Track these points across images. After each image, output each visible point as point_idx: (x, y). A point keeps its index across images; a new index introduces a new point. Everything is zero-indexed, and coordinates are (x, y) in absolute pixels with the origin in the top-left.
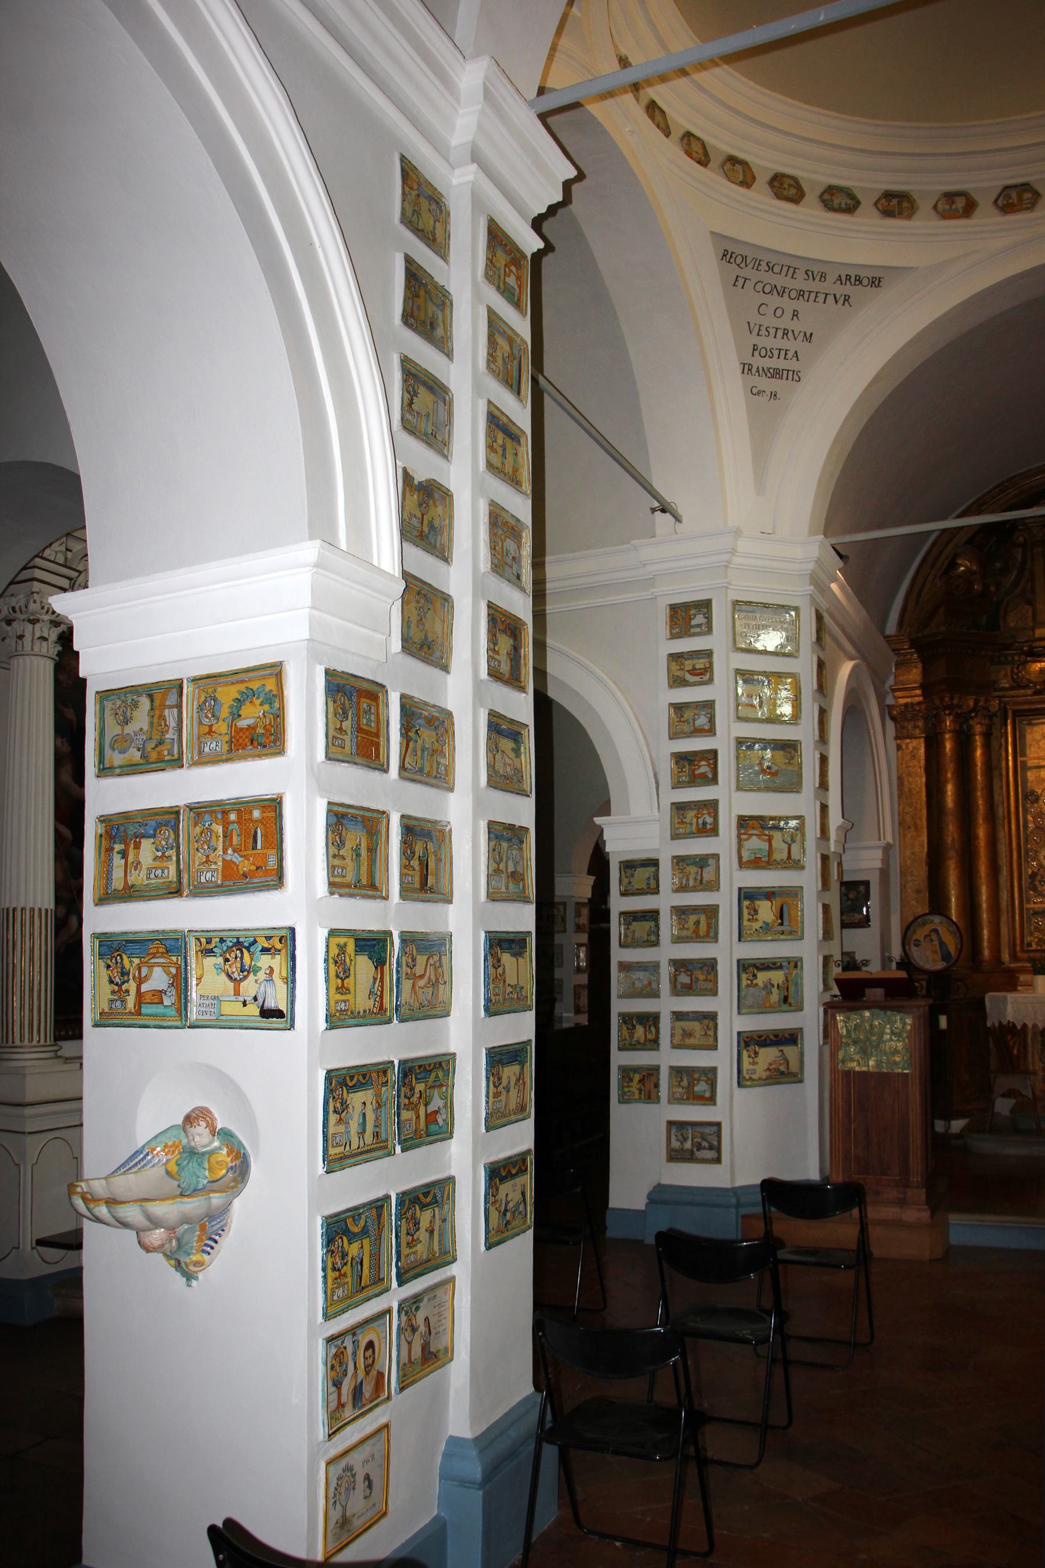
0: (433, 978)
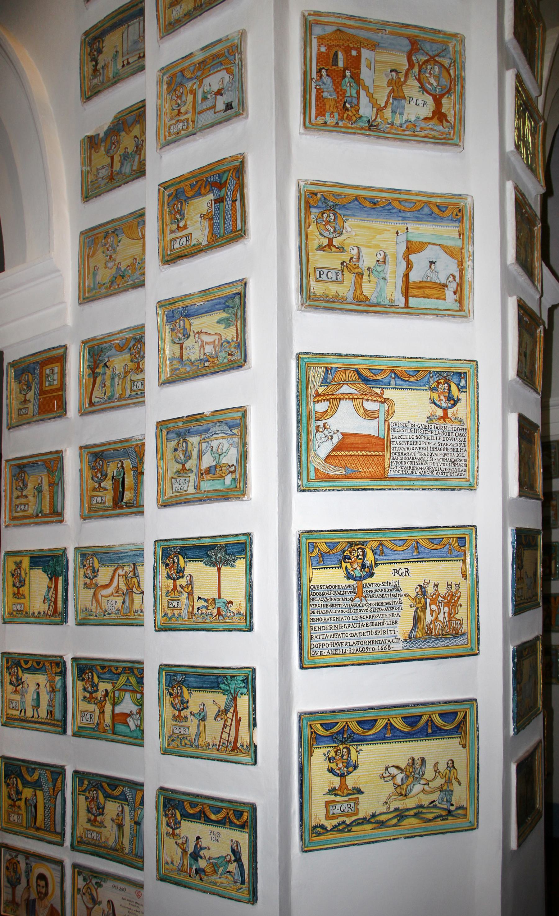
0: (123, 587)
